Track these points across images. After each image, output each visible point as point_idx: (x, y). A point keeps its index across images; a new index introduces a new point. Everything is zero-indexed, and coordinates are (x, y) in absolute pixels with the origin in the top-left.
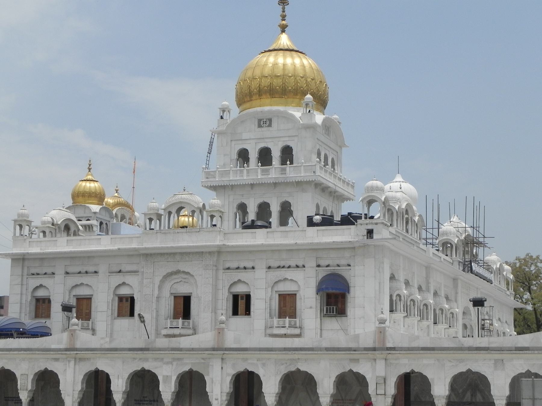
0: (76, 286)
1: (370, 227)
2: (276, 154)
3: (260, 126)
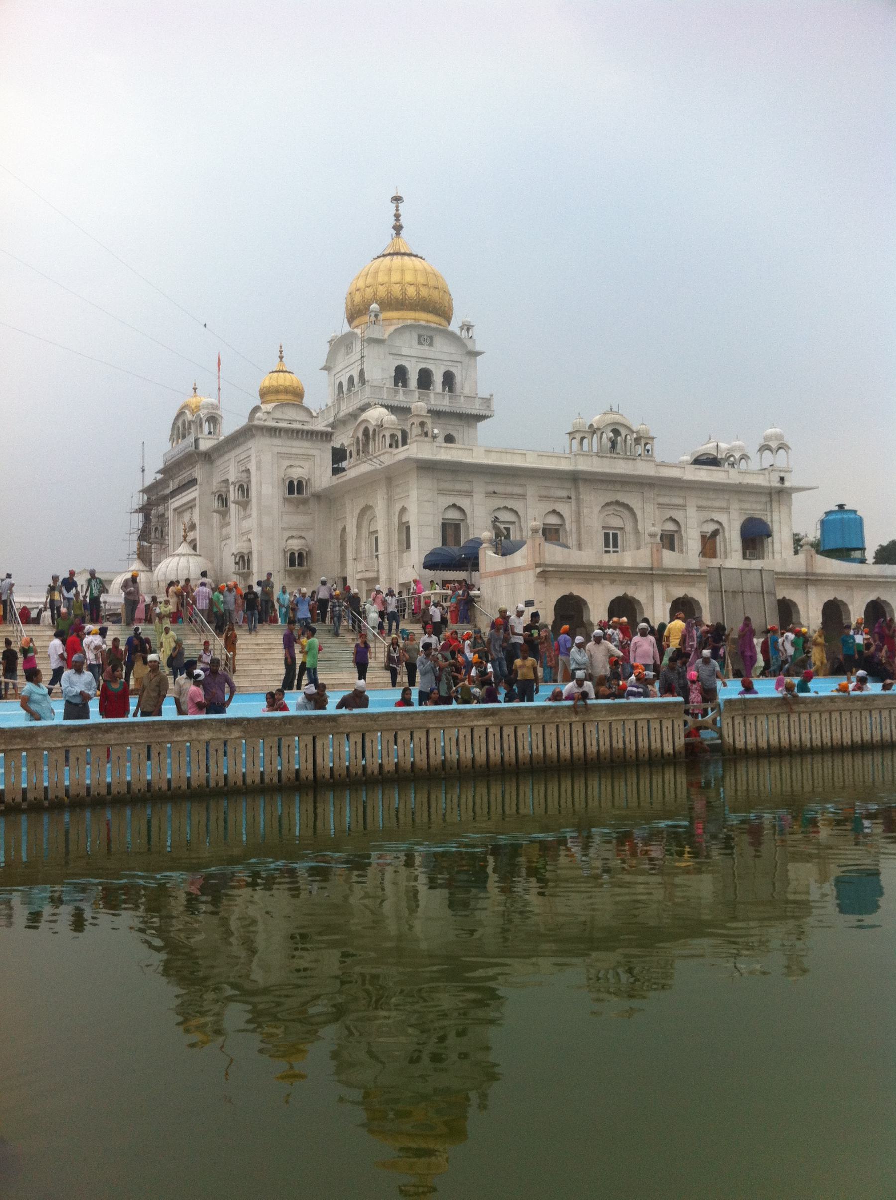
0: (499, 509)
1: (782, 474)
3: (420, 343)
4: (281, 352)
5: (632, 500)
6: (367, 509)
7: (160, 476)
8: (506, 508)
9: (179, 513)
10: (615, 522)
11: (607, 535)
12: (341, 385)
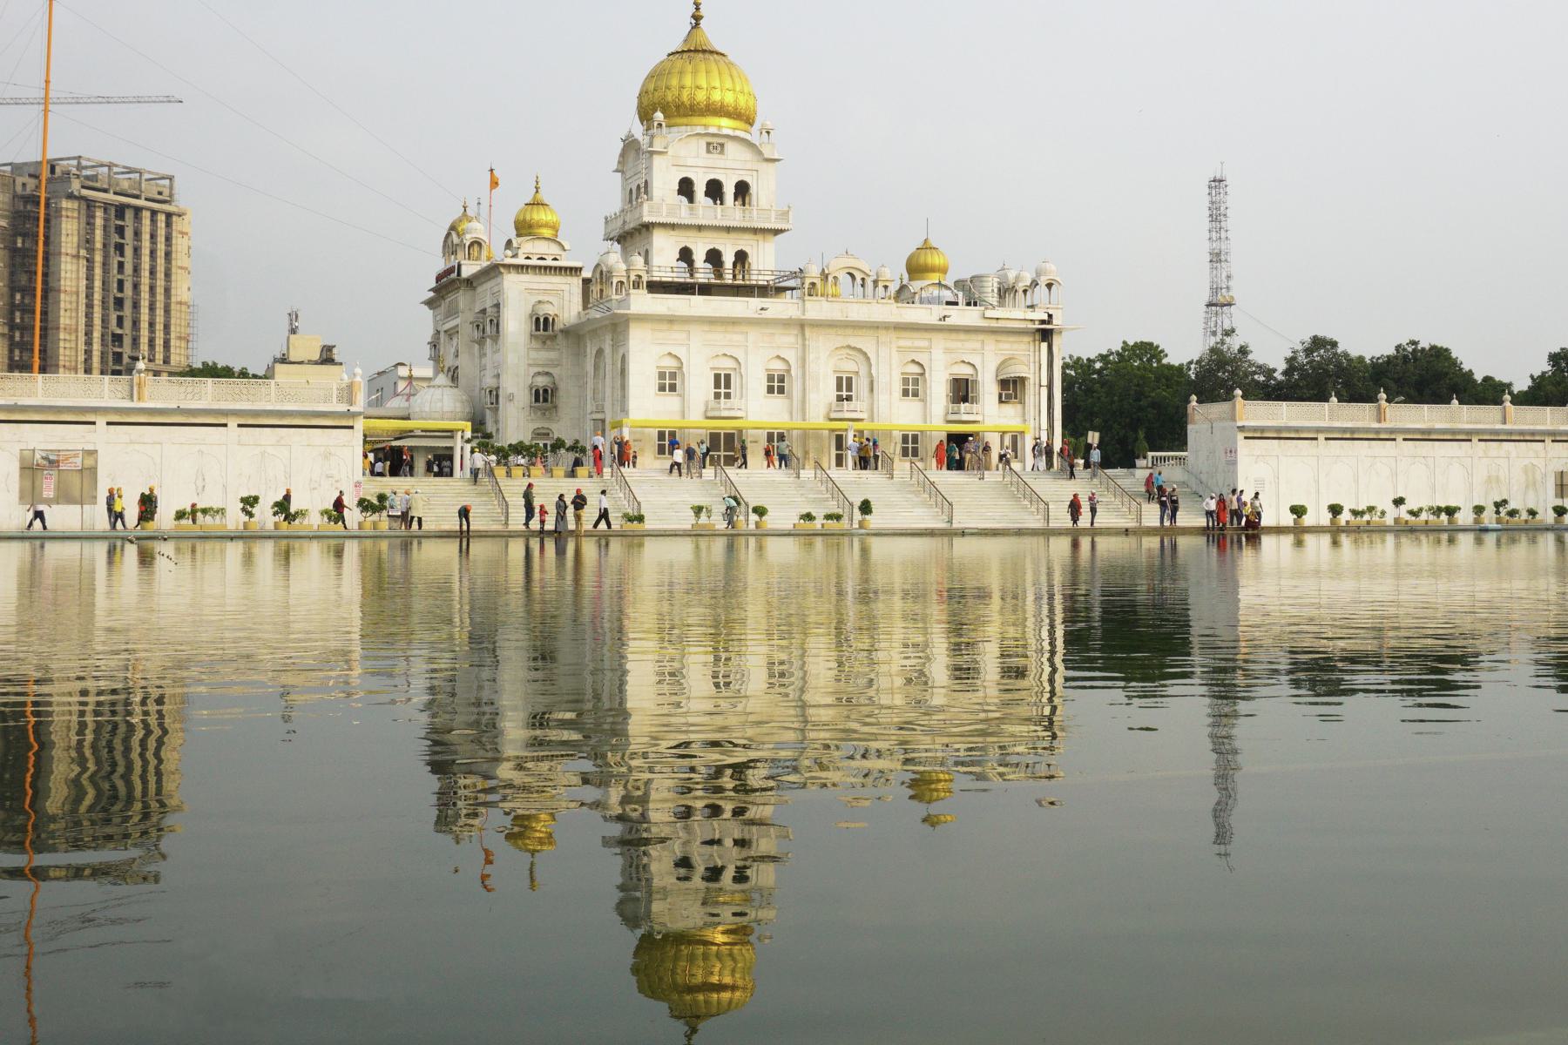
2: (729, 191)
3: (708, 151)
4: (537, 183)
5: (865, 342)
6: (600, 352)
7: (432, 294)
8: (725, 355)
9: (450, 335)
10: (849, 366)
11: (839, 380)
12: (631, 190)
